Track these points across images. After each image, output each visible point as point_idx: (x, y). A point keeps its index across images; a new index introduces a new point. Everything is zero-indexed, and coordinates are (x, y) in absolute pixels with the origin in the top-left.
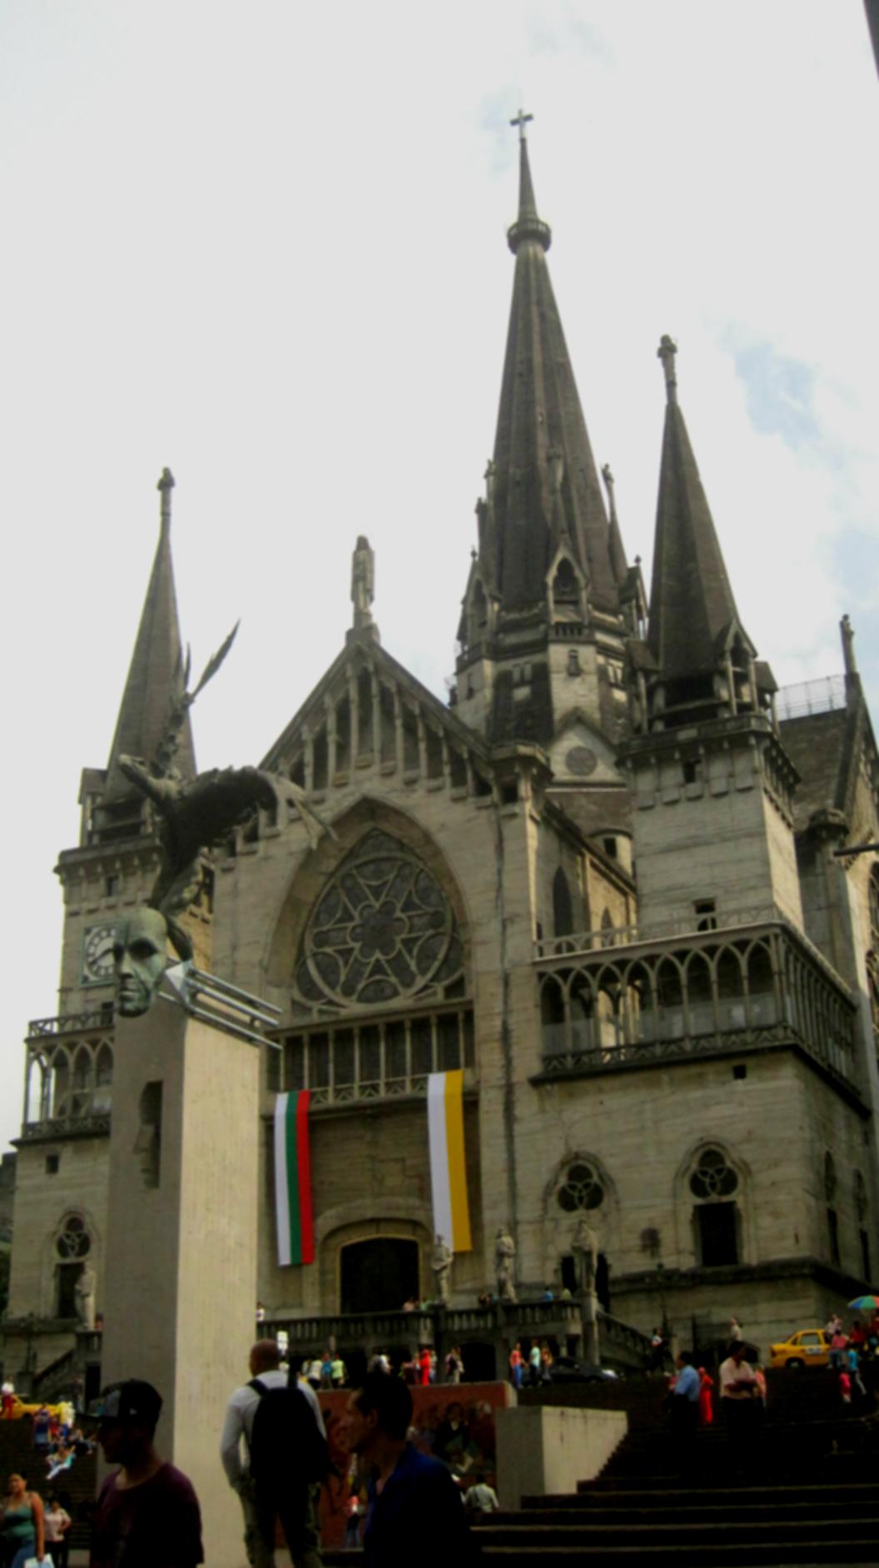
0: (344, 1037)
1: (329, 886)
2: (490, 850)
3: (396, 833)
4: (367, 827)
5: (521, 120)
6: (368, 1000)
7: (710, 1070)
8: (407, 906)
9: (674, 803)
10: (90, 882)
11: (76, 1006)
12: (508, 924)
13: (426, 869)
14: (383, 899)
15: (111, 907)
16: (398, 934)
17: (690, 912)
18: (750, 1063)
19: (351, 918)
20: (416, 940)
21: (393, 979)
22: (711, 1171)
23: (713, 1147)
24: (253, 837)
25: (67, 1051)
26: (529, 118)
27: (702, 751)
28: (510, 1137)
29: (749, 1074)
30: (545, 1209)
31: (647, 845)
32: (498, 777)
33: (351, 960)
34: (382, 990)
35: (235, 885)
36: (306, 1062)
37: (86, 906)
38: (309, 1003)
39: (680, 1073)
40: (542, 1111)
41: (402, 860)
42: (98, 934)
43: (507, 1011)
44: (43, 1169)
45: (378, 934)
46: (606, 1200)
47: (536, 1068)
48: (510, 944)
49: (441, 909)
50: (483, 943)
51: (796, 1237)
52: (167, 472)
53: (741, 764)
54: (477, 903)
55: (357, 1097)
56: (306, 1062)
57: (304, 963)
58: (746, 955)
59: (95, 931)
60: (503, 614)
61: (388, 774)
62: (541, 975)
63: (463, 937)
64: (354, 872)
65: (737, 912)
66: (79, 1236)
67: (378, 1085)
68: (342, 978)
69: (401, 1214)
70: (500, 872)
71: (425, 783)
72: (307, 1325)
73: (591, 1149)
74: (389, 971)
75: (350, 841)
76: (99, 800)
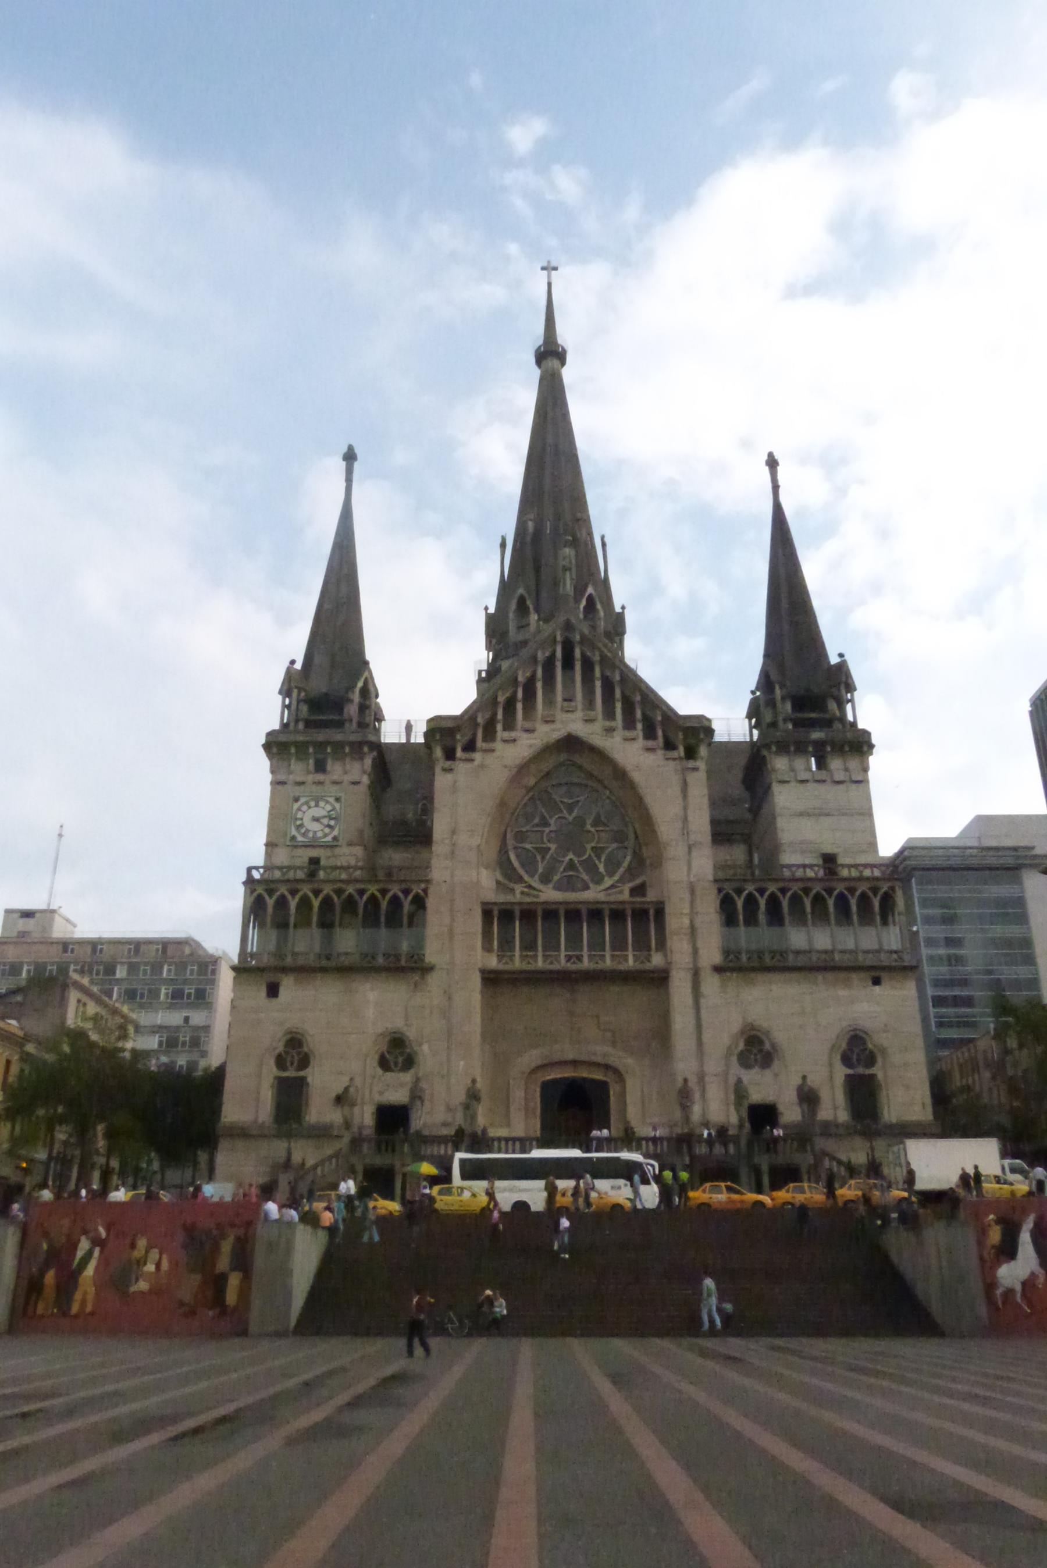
0: (551, 913)
1: (527, 798)
2: (676, 790)
3: (588, 766)
4: (563, 757)
5: (549, 268)
7: (854, 976)
8: (597, 822)
11: (282, 857)
12: (693, 849)
14: (574, 814)
15: (320, 783)
17: (820, 862)
18: (884, 975)
19: (547, 824)
20: (603, 849)
21: (585, 877)
24: (470, 747)
25: (289, 897)
27: (829, 749)
29: (883, 983)
30: (728, 1066)
32: (685, 738)
33: (548, 857)
35: (455, 782)
36: (517, 929)
39: (830, 976)
42: (307, 803)
43: (693, 914)
44: (263, 992)
45: (571, 839)
47: (717, 958)
48: (695, 863)
51: (923, 1104)
52: (351, 448)
53: (799, 763)
55: (562, 963)
56: (517, 929)
57: (507, 852)
58: (879, 898)
59: (303, 800)
60: (541, 623)
61: (588, 721)
62: (720, 890)
63: (646, 852)
64: (549, 790)
65: (850, 866)
66: (299, 1053)
67: (582, 956)
68: (540, 870)
69: (599, 1059)
70: (685, 808)
72: (510, 1143)
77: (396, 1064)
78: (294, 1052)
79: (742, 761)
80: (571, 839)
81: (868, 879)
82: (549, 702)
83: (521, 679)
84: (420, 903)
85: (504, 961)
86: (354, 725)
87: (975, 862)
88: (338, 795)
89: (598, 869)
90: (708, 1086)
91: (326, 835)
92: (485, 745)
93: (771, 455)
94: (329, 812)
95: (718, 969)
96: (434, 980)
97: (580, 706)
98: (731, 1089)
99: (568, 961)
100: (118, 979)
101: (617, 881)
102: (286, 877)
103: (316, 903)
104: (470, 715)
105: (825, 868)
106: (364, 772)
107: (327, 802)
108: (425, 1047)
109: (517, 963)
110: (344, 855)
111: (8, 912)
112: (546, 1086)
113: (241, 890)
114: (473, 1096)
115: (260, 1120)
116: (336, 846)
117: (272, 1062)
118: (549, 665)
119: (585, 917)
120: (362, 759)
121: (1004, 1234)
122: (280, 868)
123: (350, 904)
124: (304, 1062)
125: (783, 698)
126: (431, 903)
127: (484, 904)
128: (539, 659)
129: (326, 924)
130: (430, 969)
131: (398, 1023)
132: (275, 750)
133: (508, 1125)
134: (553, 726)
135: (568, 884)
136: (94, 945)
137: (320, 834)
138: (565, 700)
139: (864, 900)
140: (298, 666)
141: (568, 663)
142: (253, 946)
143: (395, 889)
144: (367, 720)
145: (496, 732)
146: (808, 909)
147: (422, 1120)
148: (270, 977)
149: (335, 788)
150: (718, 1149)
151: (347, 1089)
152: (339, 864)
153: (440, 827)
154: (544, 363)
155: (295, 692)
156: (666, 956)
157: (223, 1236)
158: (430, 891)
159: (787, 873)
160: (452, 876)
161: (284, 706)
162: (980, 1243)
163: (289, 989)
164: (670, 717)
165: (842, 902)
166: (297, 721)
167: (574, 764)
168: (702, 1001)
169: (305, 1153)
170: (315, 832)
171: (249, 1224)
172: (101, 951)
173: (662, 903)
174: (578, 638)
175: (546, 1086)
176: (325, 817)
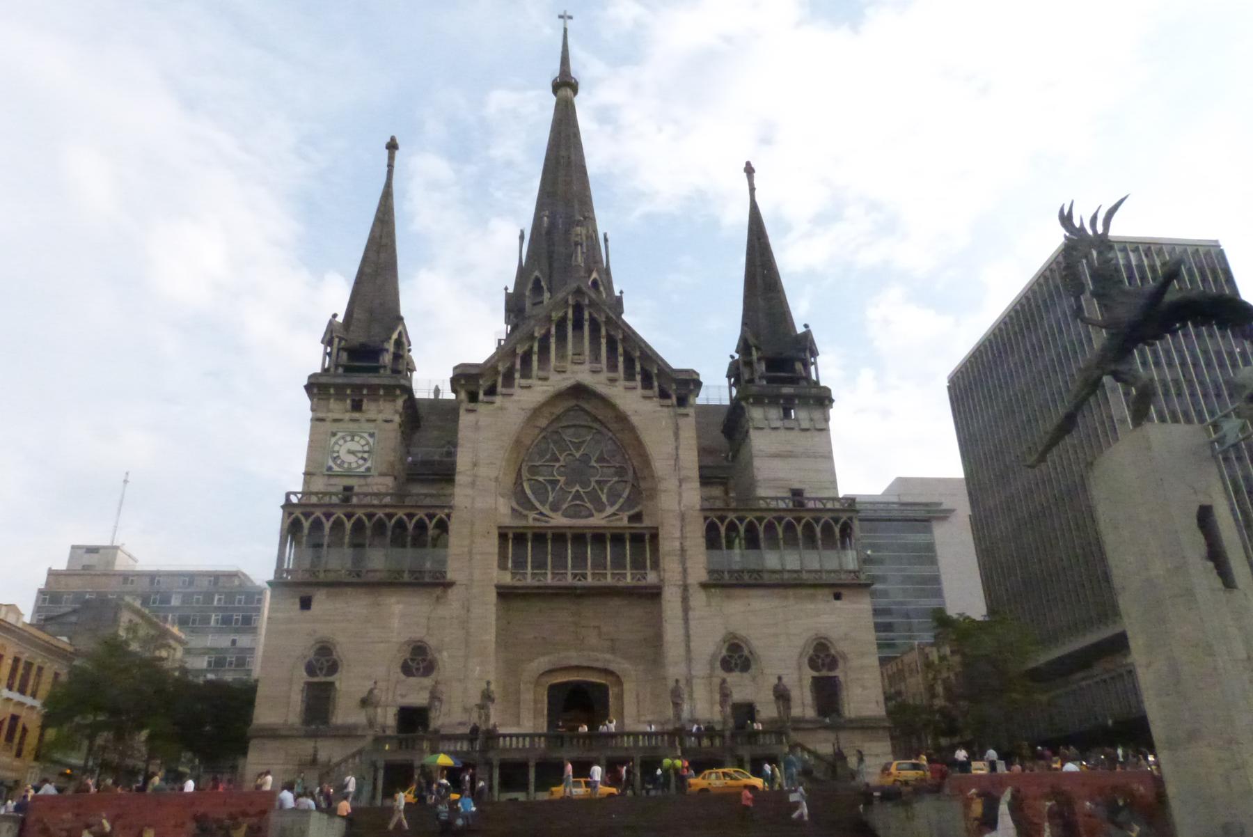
0: (559, 537)
1: (540, 437)
2: (671, 433)
3: (594, 412)
4: (572, 403)
6: (566, 517)
7: (820, 592)
9: (776, 429)
10: (336, 400)
11: (319, 485)
13: (614, 437)
14: (581, 452)
15: (356, 421)
16: (593, 476)
17: (789, 495)
18: (844, 592)
19: (557, 460)
20: (607, 482)
21: (588, 505)
22: (822, 655)
23: (823, 641)
24: (491, 391)
25: (324, 519)
26: (570, 18)
27: (797, 402)
28: (686, 620)
29: (843, 598)
30: (712, 668)
31: (760, 451)
34: (580, 512)
37: (331, 416)
38: (525, 512)
40: (709, 605)
41: (596, 429)
42: (343, 438)
43: (683, 537)
44: (298, 606)
46: (753, 666)
47: (704, 576)
48: (685, 495)
49: (625, 466)
50: (665, 491)
51: (877, 702)
52: (393, 139)
54: (661, 465)
55: (569, 580)
58: (839, 526)
59: (340, 435)
61: (594, 372)
62: (706, 518)
63: (643, 485)
64: (560, 430)
65: (815, 499)
66: (328, 661)
67: (586, 574)
68: (551, 499)
70: (677, 448)
71: (622, 383)
73: (742, 632)
74: (586, 500)
75: (559, 410)
76: (343, 343)
77: (418, 669)
78: (323, 659)
79: (721, 419)
80: (578, 473)
81: (829, 510)
82: (562, 356)
83: (536, 334)
84: (443, 526)
85: (518, 578)
86: (389, 372)
87: (896, 514)
88: (372, 431)
89: (601, 499)
90: (694, 688)
91: (359, 466)
92: (505, 391)
93: (748, 164)
94: (363, 446)
95: (704, 586)
96: (452, 593)
97: (587, 358)
98: (717, 688)
99: (574, 578)
100: (173, 607)
101: (617, 510)
102: (322, 502)
103: (348, 525)
104: (490, 367)
105: (794, 502)
106: (396, 412)
107: (362, 437)
108: (445, 654)
109: (529, 581)
110: (377, 484)
111: (74, 547)
112: (553, 689)
113: (280, 512)
114: (487, 697)
115: (290, 721)
116: (369, 476)
117: (303, 668)
118: (561, 324)
119: (589, 540)
120: (394, 401)
121: (985, 807)
122: (316, 494)
123: (380, 527)
124: (333, 668)
125: (759, 359)
126: (453, 526)
127: (500, 528)
128: (553, 319)
129: (357, 546)
130: (451, 584)
131: (419, 633)
132: (315, 391)
133: (518, 724)
134: (564, 376)
135: (574, 512)
136: (153, 577)
137: (354, 465)
138: (574, 354)
139: (827, 529)
140: (340, 319)
141: (578, 326)
142: (289, 563)
143: (421, 514)
144: (401, 367)
145: (514, 379)
146: (781, 535)
147: (441, 720)
148: (306, 591)
149: (372, 425)
150: (705, 742)
151: (371, 692)
152: (371, 491)
153: (463, 460)
154: (558, 94)
155: (336, 340)
156: (659, 576)
157: (237, 826)
158: (452, 515)
159: (762, 504)
160: (473, 503)
161: (326, 354)
162: (966, 816)
163: (322, 603)
164: (665, 371)
165: (809, 528)
166: (337, 366)
167: (583, 410)
168: (691, 614)
169: (330, 751)
170: (350, 463)
171: (263, 812)
172: (159, 581)
173: (657, 528)
174: (587, 301)
175: (553, 689)
176: (359, 452)
